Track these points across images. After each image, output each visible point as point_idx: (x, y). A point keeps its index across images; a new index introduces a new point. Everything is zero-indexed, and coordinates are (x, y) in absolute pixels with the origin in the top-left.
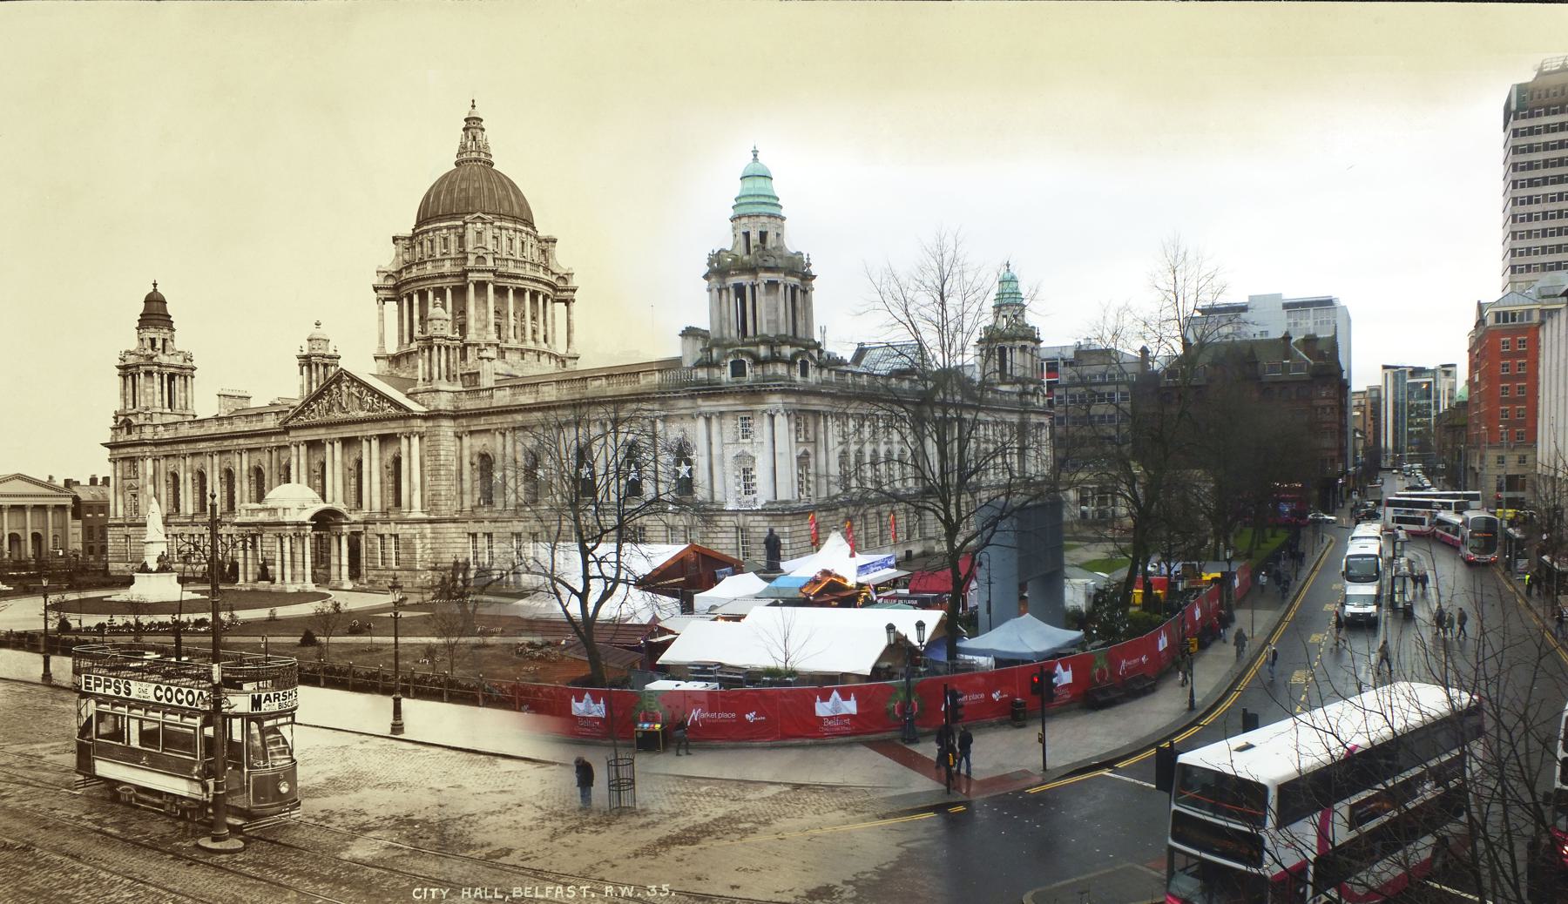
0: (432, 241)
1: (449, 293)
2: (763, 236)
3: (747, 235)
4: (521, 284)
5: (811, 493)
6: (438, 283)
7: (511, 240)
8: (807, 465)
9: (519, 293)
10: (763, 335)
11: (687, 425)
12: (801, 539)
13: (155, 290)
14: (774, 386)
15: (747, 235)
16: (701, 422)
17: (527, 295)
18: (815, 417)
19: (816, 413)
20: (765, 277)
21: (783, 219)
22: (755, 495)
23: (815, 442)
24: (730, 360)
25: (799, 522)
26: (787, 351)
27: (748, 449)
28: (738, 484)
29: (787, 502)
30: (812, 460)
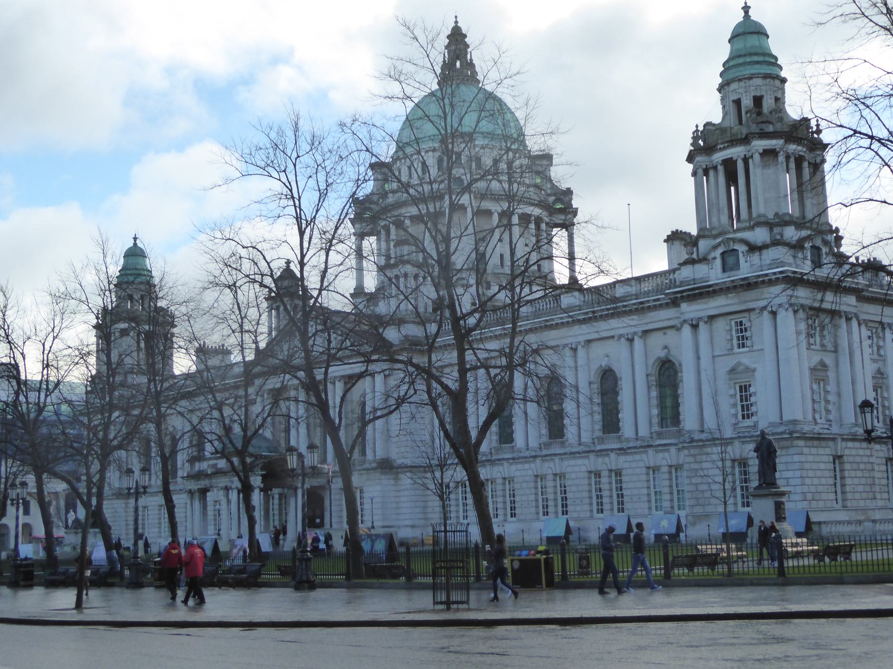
2: (758, 101)
3: (738, 102)
5: (831, 417)
10: (759, 216)
11: (670, 338)
12: (819, 473)
13: (135, 244)
14: (775, 273)
16: (687, 330)
20: (760, 145)
21: (784, 81)
22: (754, 418)
23: (836, 351)
24: (720, 250)
25: (814, 451)
26: (791, 233)
27: (746, 361)
29: (795, 422)
30: (831, 374)
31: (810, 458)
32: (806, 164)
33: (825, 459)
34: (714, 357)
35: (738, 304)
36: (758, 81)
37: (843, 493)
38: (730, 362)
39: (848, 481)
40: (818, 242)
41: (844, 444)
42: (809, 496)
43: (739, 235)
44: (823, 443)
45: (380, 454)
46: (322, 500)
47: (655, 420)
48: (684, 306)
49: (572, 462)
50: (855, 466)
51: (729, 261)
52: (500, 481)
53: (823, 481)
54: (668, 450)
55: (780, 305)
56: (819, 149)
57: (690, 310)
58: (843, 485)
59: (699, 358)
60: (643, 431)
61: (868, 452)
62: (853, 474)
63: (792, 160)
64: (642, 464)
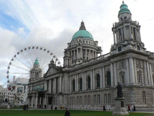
0: (73, 43)
1: (74, 51)
3: (121, 18)
4: (88, 49)
5: (142, 83)
6: (73, 50)
7: (87, 41)
8: (141, 75)
9: (88, 50)
15: (121, 18)
17: (90, 51)
18: (143, 62)
19: (143, 60)
20: (125, 25)
22: (125, 83)
23: (143, 68)
25: (138, 90)
27: (123, 70)
28: (121, 80)
30: (142, 74)
31: (137, 92)
32: (136, 30)
33: (141, 92)
34: (117, 70)
35: (121, 58)
36: (126, 14)
37: (145, 100)
38: (120, 71)
39: (146, 97)
40: (139, 45)
41: (145, 89)
42: (136, 101)
43: (121, 44)
44: (140, 88)
45: (60, 91)
46: (52, 99)
47: (106, 84)
48: (111, 60)
49: (91, 93)
50: (148, 94)
51: (120, 49)
52: (79, 97)
53: (140, 97)
54: (108, 90)
55: (130, 57)
56: (139, 27)
57: (112, 60)
58: (145, 98)
59: (114, 70)
60: (104, 87)
61: (151, 91)
62: (148, 96)
63: (133, 28)
64: (103, 93)
